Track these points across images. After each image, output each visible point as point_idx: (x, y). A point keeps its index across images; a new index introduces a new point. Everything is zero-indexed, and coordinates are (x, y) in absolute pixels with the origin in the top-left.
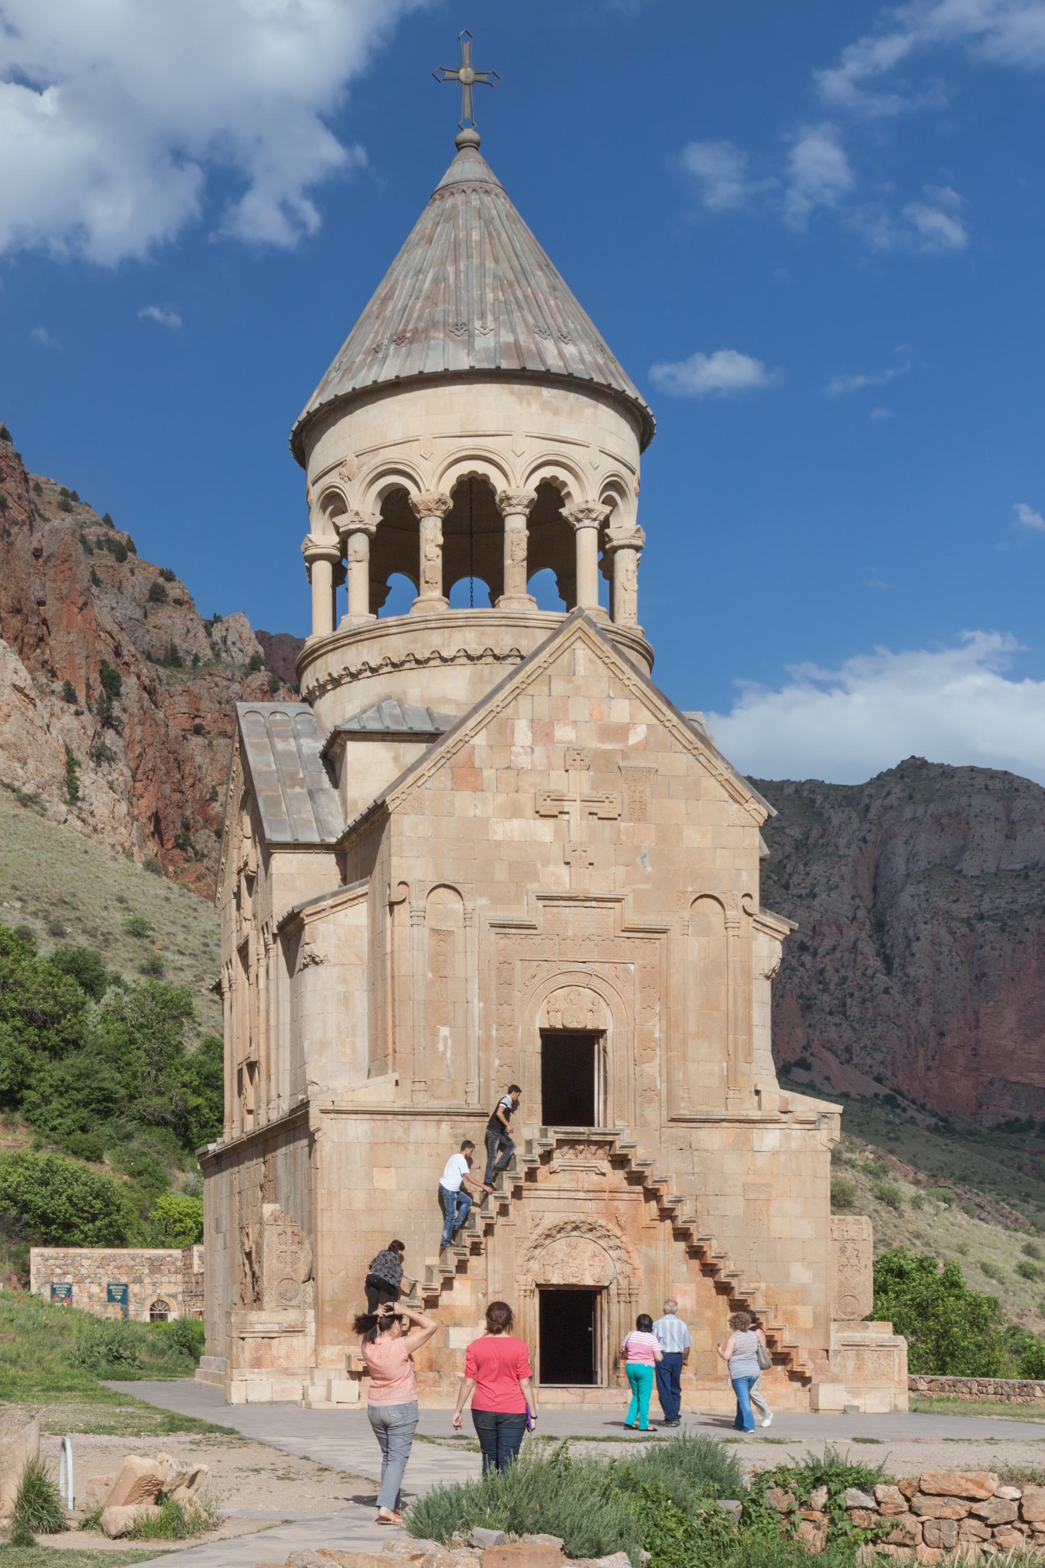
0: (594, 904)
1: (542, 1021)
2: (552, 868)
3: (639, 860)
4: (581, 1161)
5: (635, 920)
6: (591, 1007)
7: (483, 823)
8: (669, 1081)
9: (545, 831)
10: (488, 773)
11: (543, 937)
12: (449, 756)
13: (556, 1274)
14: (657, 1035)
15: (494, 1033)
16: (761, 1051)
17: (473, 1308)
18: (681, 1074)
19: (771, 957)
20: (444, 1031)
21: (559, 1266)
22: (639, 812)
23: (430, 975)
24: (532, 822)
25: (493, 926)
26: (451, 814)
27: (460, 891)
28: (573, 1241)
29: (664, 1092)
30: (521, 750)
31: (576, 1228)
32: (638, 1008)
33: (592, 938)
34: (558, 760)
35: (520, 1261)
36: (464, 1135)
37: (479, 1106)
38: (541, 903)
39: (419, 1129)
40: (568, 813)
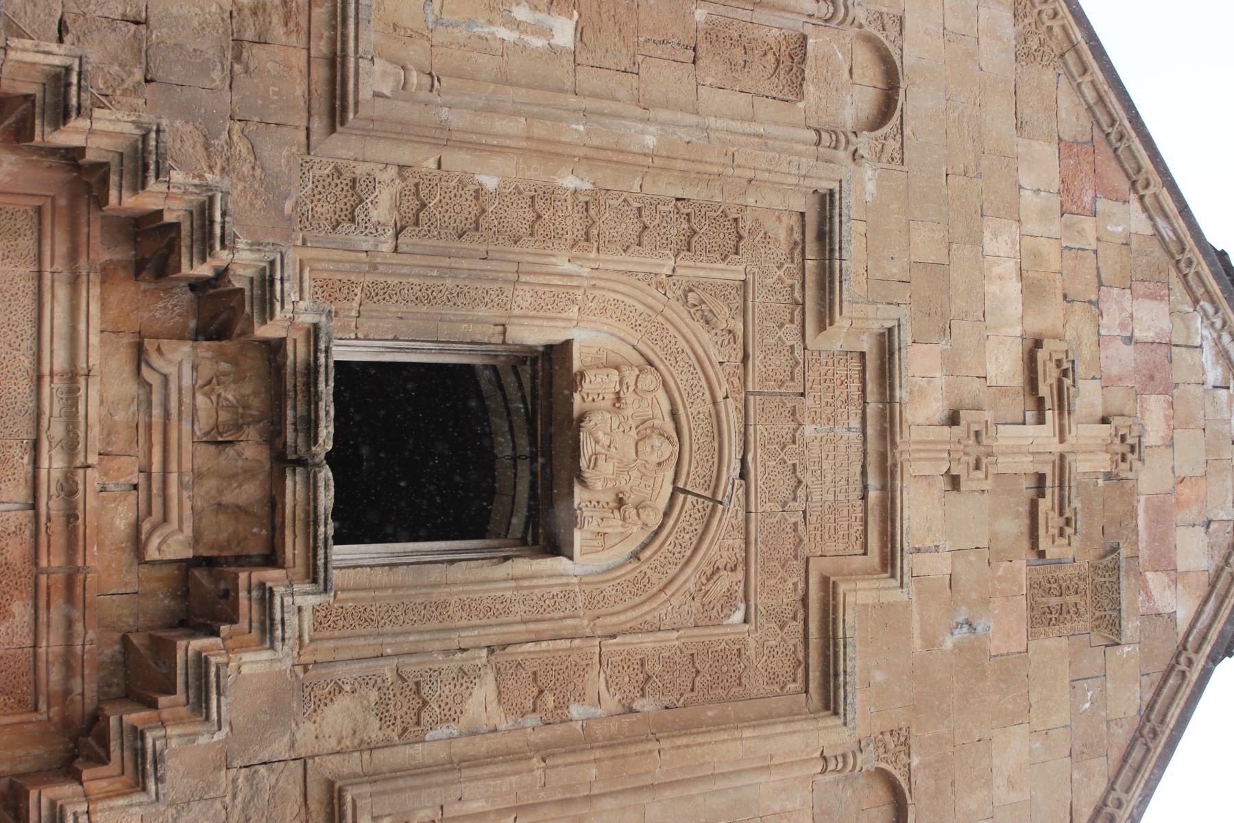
0: (873, 495)
1: (588, 340)
2: (940, 380)
4: (189, 454)
6: (631, 499)
8: (456, 765)
9: (1004, 365)
11: (798, 352)
14: (575, 711)
20: (563, 31)
22: (1044, 616)
24: (1018, 331)
26: (1019, 127)
27: (886, 129)
29: (418, 753)
32: (646, 642)
33: (801, 492)
34: (1119, 399)
36: (261, 41)
37: (365, 94)
38: (867, 345)
40: (1041, 421)
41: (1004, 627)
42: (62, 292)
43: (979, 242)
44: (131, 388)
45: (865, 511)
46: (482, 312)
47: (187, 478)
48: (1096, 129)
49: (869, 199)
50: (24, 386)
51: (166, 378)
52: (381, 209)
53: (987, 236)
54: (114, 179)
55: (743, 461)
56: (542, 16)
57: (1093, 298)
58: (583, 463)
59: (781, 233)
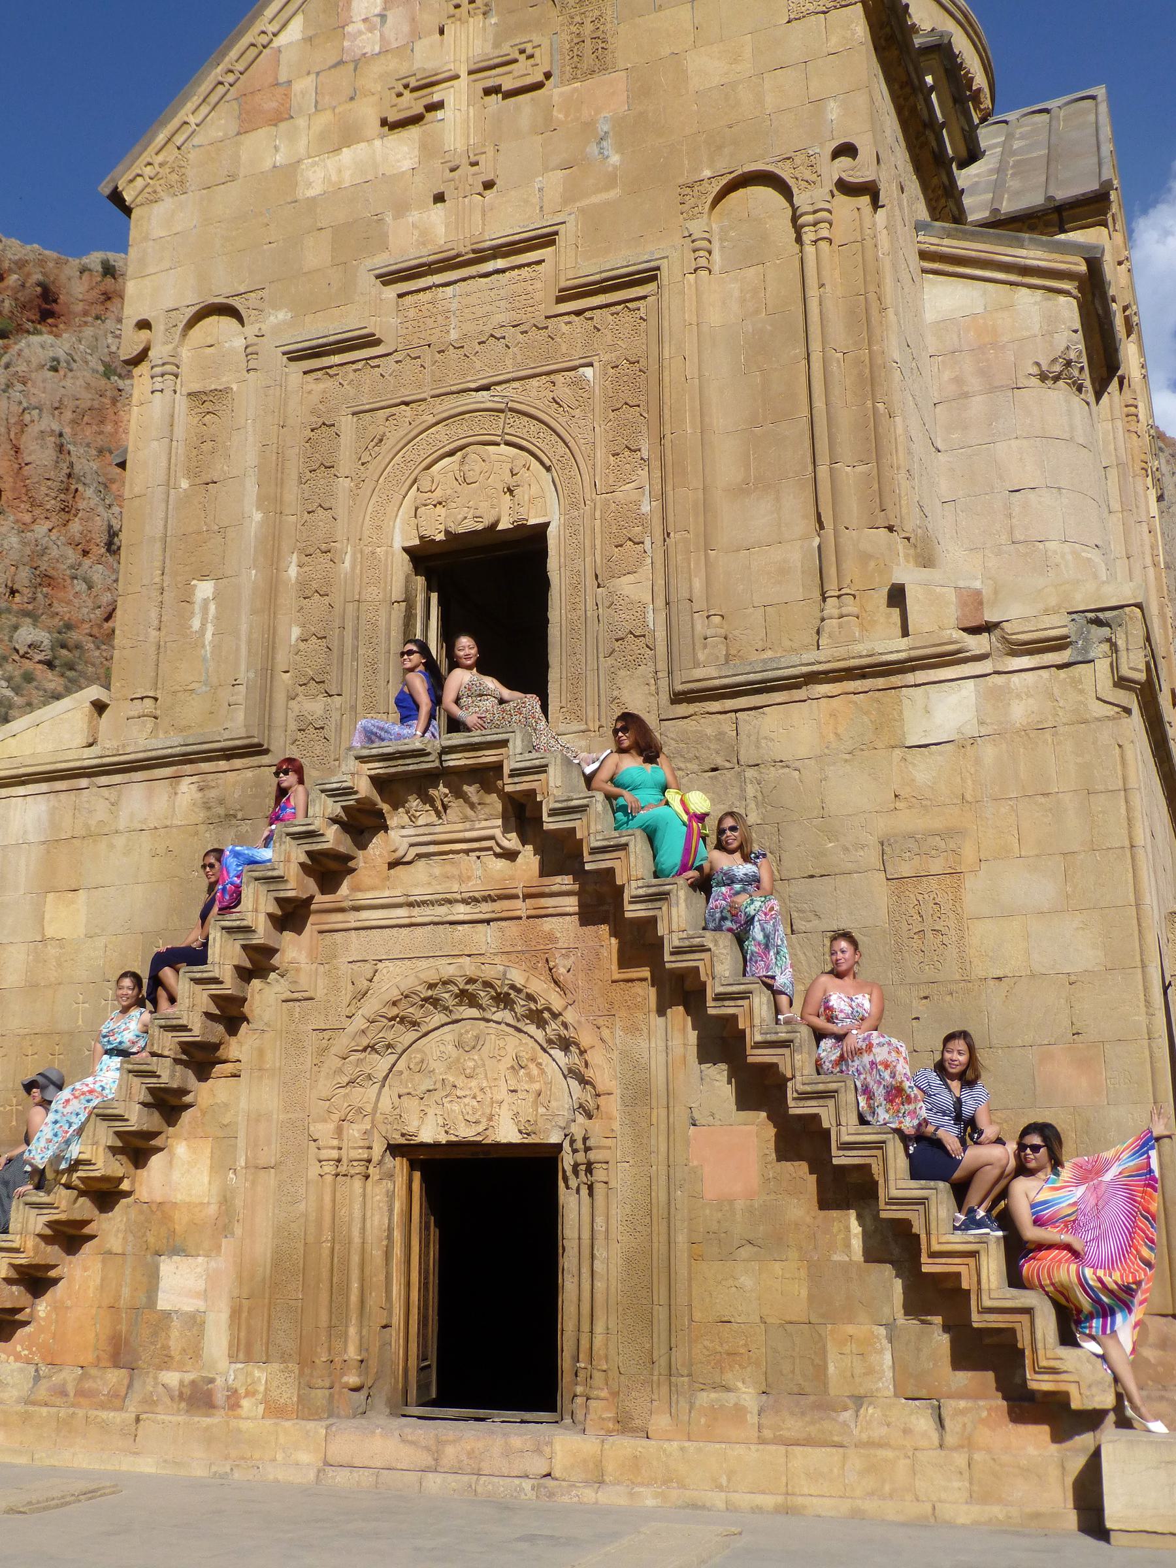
0: (500, 263)
2: (414, 216)
3: (593, 149)
5: (571, 262)
7: (289, 173)
9: (401, 151)
10: (304, 86)
12: (231, 78)
13: (430, 1120)
14: (645, 508)
15: (293, 571)
16: (1052, 546)
17: (213, 1210)
18: (698, 584)
19: (1051, 333)
20: (204, 589)
21: (437, 1096)
23: (184, 484)
24: (377, 143)
25: (295, 356)
26: (232, 178)
28: (469, 1031)
29: (661, 634)
30: (362, 26)
31: (467, 997)
35: (324, 1086)
38: (391, 292)
39: (139, 801)
41: (607, 98)
42: (365, 914)
43: (314, 198)
44: (421, 863)
45: (512, 268)
46: (382, 623)
47: (468, 825)
48: (227, 97)
49: (289, 315)
50: (420, 930)
51: (412, 845)
52: (315, 707)
53: (311, 193)
54: (282, 894)
55: (477, 390)
56: (197, 608)
57: (352, 66)
58: (480, 527)
59: (318, 387)
